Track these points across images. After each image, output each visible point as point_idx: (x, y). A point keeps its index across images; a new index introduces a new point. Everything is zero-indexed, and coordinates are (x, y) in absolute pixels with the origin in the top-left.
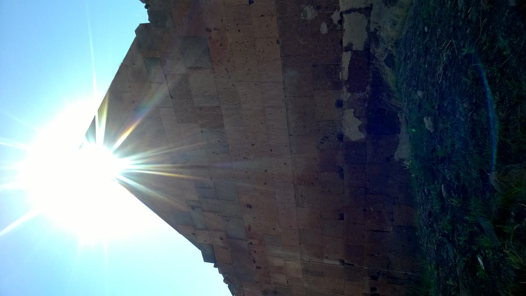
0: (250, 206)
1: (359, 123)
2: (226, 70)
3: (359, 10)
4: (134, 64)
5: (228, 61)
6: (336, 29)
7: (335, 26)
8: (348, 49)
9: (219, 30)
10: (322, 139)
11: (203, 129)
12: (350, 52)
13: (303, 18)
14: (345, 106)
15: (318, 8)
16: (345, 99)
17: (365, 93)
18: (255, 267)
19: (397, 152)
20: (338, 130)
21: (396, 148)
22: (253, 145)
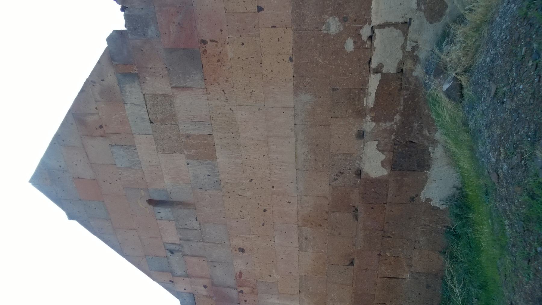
0: (242, 250)
1: (382, 157)
2: (223, 91)
3: (396, 25)
4: (102, 80)
6: (365, 47)
7: (364, 43)
8: (377, 71)
9: (217, 42)
10: (337, 175)
11: (189, 161)
12: (379, 75)
13: (325, 32)
14: (367, 137)
15: (344, 20)
16: (368, 130)
17: (393, 123)
19: (423, 191)
20: (356, 165)
21: (424, 186)
22: (251, 180)
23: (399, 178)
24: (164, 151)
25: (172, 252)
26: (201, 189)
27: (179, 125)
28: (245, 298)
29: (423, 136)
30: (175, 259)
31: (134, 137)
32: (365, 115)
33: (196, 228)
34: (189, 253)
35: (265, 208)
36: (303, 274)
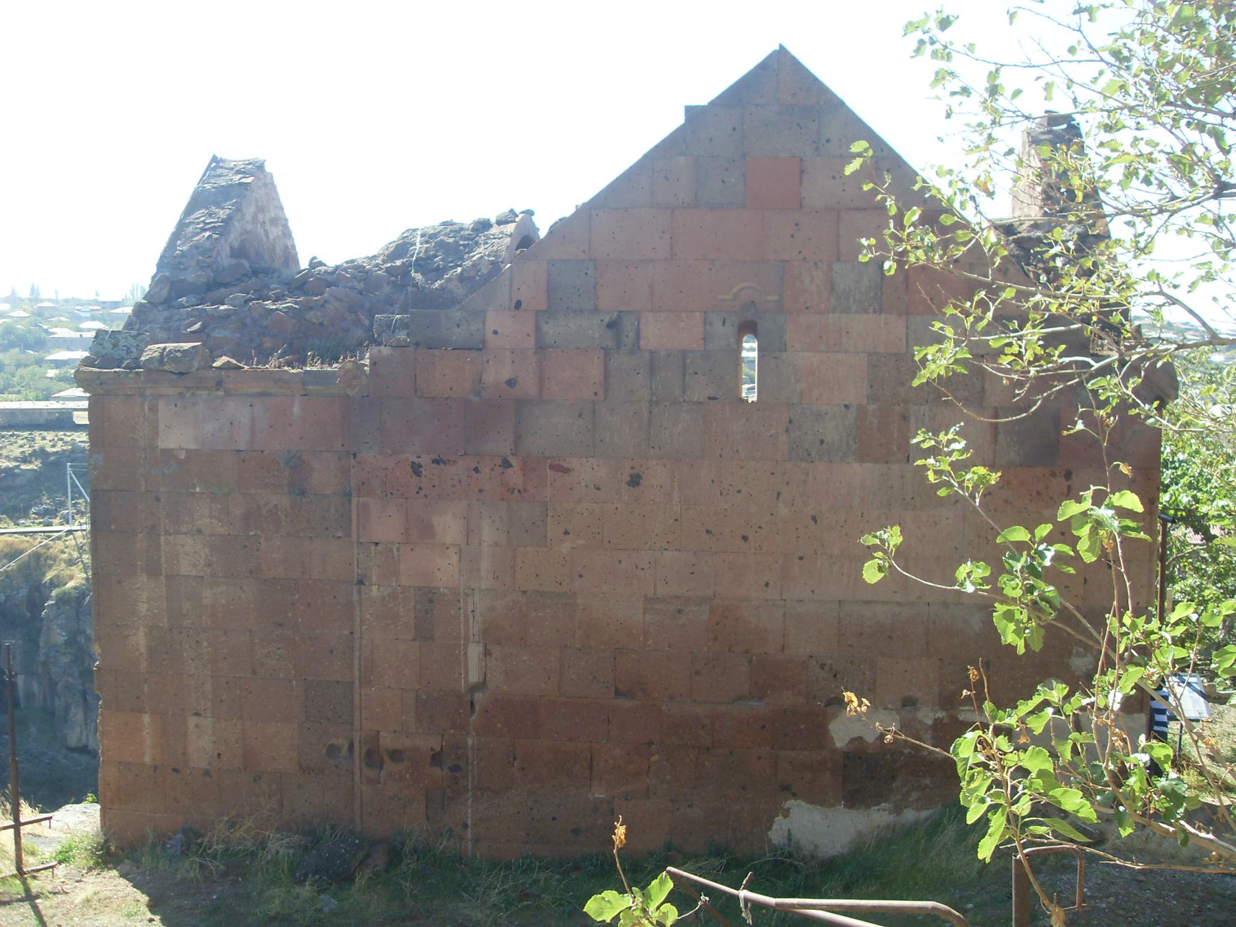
0: (635, 481)
16: (920, 715)
18: (416, 460)
21: (812, 803)
23: (829, 765)
25: (611, 325)
26: (791, 422)
31: (900, 315)
32: (946, 710)
35: (751, 537)
36: (580, 601)
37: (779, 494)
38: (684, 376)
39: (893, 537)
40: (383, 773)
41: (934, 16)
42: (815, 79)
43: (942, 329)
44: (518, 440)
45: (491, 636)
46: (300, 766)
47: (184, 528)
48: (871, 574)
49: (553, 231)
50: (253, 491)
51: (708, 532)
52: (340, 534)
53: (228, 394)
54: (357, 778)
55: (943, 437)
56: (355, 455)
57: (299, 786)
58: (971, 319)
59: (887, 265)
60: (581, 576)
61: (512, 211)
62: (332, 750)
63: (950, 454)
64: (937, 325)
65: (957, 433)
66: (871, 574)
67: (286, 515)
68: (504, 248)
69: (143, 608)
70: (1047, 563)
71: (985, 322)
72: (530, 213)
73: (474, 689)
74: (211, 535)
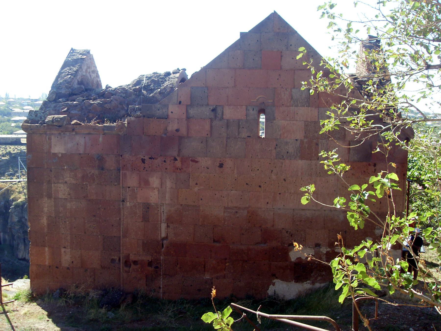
0: (221, 166)
5: (353, 174)
11: (299, 141)
16: (321, 250)
18: (143, 158)
22: (285, 180)
24: (306, 126)
25: (213, 110)
26: (277, 145)
27: (325, 140)
28: (168, 162)
29: (317, 277)
30: (206, 111)
31: (316, 108)
33: (240, 134)
34: (214, 124)
35: (262, 186)
36: (201, 208)
37: (272, 171)
38: (239, 128)
39: (312, 188)
40: (131, 269)
41: (328, 4)
42: (287, 23)
43: (330, 114)
44: (179, 150)
45: (169, 220)
46: (101, 266)
47: (60, 181)
48: (304, 201)
49: (192, 76)
50: (85, 168)
51: (247, 184)
52: (116, 184)
53: (76, 133)
54: (122, 271)
55: (330, 153)
56: (121, 156)
57: (101, 273)
58: (340, 111)
59: (311, 91)
60: (201, 199)
61: (178, 69)
62: (113, 261)
63: (332, 159)
64: (328, 113)
65: (335, 152)
66: (304, 201)
67: (97, 177)
68: (175, 82)
69: (46, 209)
70: (366, 198)
71: (345, 112)
72: (184, 70)
73: (163, 239)
74: (70, 184)
